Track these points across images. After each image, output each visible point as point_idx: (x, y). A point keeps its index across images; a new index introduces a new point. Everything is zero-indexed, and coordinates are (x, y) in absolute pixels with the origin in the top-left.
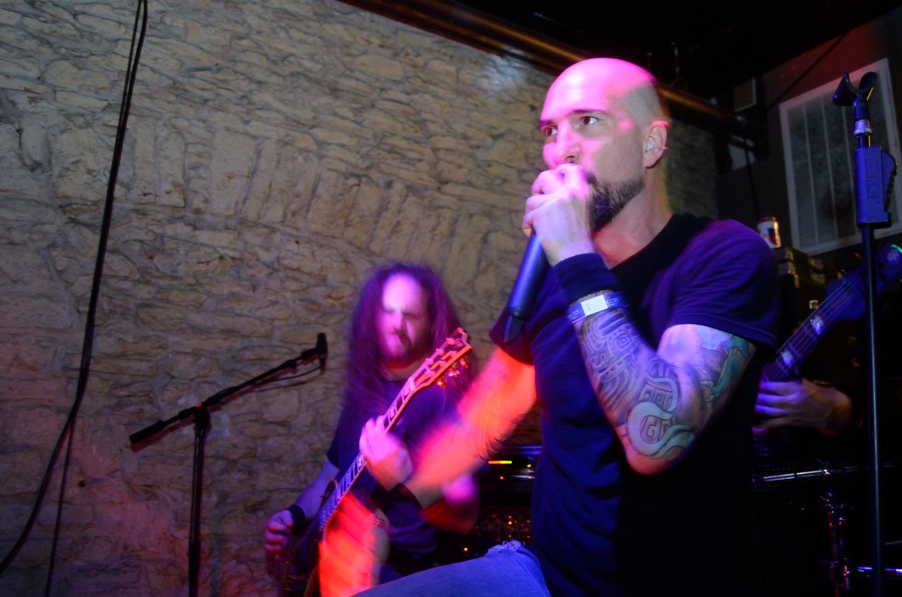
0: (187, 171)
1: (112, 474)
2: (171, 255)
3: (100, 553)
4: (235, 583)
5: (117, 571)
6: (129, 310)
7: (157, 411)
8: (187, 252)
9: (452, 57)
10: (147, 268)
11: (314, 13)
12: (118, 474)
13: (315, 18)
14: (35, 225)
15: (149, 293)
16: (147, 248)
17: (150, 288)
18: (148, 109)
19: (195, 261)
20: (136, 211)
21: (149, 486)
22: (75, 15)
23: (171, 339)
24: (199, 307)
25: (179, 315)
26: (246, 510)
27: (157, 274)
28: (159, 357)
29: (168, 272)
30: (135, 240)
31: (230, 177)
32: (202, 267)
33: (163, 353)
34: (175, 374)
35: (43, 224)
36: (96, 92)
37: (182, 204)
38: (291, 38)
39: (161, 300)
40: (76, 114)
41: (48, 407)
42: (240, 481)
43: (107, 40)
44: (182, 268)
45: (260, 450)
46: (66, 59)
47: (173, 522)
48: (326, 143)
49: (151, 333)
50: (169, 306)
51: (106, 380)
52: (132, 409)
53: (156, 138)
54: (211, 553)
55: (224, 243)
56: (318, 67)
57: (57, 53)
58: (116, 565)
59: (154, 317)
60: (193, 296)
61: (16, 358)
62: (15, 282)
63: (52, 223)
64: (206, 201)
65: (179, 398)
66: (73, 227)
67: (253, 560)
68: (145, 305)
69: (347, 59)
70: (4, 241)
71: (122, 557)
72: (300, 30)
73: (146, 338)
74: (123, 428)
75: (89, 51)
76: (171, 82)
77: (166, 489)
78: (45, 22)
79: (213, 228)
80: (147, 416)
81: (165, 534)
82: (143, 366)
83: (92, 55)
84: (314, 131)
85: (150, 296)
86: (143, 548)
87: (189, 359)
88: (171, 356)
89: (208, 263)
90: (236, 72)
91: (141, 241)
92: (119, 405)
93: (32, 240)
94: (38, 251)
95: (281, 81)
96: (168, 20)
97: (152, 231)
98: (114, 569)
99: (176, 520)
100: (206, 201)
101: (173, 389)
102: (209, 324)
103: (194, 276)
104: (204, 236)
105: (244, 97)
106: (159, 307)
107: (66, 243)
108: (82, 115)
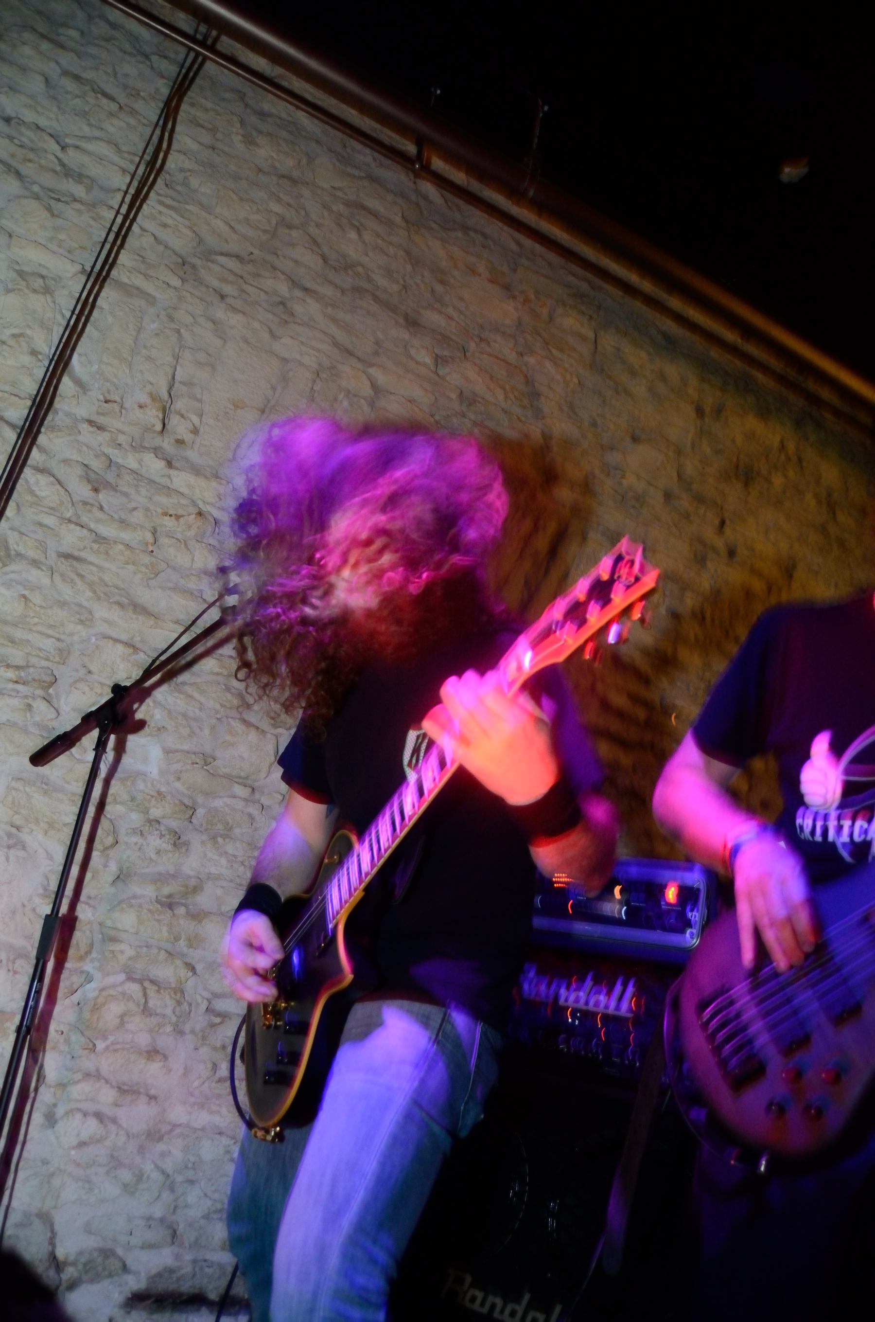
0: (177, 385)
2: (126, 495)
4: (113, 1011)
7: (53, 714)
9: (591, 317)
11: (403, 217)
13: (404, 224)
15: (81, 539)
16: (92, 475)
18: (138, 289)
19: (160, 511)
20: (91, 422)
21: (18, 828)
22: (63, 148)
26: (158, 901)
31: (236, 407)
32: (169, 522)
36: (69, 252)
37: (159, 427)
38: (364, 242)
40: (34, 274)
43: (102, 188)
44: (137, 518)
45: (201, 812)
46: (37, 197)
47: (41, 891)
48: (387, 391)
53: (140, 330)
54: (88, 953)
55: (209, 496)
56: (395, 288)
57: (26, 188)
64: (195, 431)
67: (152, 982)
69: (439, 288)
72: (378, 235)
73: (62, 604)
75: (72, 195)
76: (180, 260)
77: (40, 837)
78: (21, 146)
79: (197, 471)
80: (37, 718)
81: (24, 906)
82: (48, 644)
83: (75, 200)
84: (372, 371)
88: (93, 639)
89: (178, 517)
90: (275, 269)
95: (339, 294)
96: (194, 182)
100: (195, 431)
101: (87, 689)
103: (154, 532)
104: (181, 480)
105: (282, 303)
108: (43, 277)
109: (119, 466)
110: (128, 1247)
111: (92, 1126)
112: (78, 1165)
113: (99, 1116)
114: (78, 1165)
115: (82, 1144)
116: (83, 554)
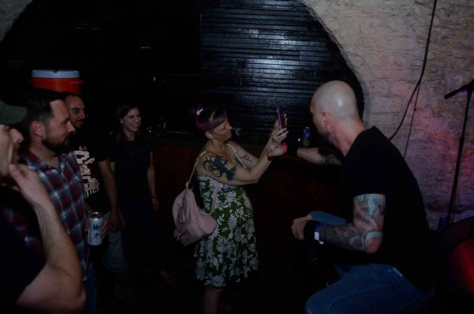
1: (427, 106)
2: (457, 14)
3: (420, 135)
4: (469, 152)
5: (426, 142)
6: (438, 40)
8: (464, 13)
10: (447, 21)
12: (429, 107)
14: (402, 6)
15: (447, 32)
17: (447, 30)
23: (454, 51)
25: (458, 41)
27: (451, 23)
28: (448, 60)
29: (456, 22)
30: (442, 8)
32: (470, 18)
33: (450, 58)
34: (454, 67)
35: (405, 6)
39: (452, 35)
41: (404, 80)
44: (462, 19)
49: (445, 50)
50: (454, 37)
51: (427, 70)
52: (437, 81)
58: (425, 140)
59: (448, 43)
60: (466, 32)
61: (394, 62)
62: (394, 31)
63: (408, 5)
65: (455, 77)
66: (417, 6)
68: (444, 38)
70: (391, 15)
71: (428, 138)
74: (432, 89)
82: (442, 64)
85: (447, 33)
87: (461, 60)
88: (453, 59)
91: (444, 9)
92: (431, 80)
93: (400, 13)
94: (403, 17)
97: (449, 3)
98: (425, 142)
99: (449, 125)
103: (467, 23)
106: (450, 38)
107: (414, 13)
109: (453, 5)
111: (466, 178)
112: (464, 186)
114: (464, 186)
115: (464, 182)
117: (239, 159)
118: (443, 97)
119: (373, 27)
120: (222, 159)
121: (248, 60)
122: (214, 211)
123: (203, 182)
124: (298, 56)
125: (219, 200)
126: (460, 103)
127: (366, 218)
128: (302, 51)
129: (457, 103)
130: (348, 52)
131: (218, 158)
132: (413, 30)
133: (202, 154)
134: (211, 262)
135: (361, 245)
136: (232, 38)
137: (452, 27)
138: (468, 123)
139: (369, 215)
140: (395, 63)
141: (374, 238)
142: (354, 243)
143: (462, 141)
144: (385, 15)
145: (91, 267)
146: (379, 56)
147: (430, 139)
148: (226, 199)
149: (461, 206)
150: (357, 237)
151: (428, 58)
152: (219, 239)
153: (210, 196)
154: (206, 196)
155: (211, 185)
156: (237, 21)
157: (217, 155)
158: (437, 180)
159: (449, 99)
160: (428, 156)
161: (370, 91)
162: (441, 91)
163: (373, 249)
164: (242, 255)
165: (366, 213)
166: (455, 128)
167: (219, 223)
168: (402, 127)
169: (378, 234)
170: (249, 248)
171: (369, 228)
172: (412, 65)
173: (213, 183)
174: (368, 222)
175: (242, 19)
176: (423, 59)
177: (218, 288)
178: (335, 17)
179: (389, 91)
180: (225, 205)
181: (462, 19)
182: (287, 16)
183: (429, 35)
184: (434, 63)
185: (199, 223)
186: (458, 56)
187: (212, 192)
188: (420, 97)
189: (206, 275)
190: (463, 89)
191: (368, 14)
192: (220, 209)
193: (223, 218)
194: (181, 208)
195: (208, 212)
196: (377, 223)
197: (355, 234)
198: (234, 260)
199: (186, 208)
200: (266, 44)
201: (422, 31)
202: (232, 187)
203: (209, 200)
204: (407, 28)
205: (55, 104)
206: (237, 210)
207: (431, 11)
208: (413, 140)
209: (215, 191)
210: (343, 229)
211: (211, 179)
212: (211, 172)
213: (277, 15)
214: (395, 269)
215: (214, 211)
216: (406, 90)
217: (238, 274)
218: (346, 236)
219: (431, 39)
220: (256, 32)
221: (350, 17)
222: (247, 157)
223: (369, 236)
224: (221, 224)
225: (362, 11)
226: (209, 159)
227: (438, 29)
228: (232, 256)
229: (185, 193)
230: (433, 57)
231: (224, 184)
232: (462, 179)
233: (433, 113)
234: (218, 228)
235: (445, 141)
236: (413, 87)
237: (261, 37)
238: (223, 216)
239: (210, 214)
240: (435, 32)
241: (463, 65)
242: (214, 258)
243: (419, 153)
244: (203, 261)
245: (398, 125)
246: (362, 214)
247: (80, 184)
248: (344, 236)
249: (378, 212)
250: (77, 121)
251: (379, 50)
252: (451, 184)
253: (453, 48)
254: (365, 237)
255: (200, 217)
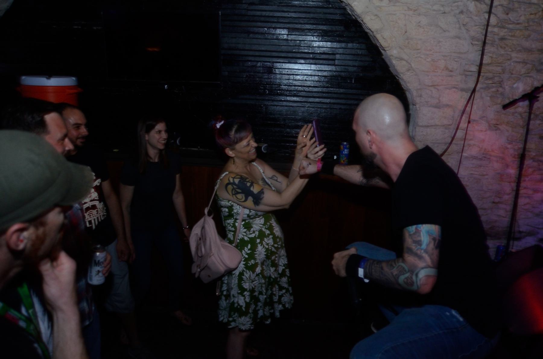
1: (482, 118)
3: (474, 151)
4: (531, 170)
5: (481, 159)
14: (454, 3)
15: (505, 32)
17: (506, 30)
23: (514, 55)
24: (527, 37)
27: (510, 22)
29: (516, 22)
30: (499, 5)
32: (532, 16)
34: (514, 72)
39: (512, 36)
41: (456, 88)
42: (539, 124)
49: (503, 52)
50: (513, 38)
51: (483, 76)
52: (494, 90)
59: (507, 45)
60: (527, 33)
62: (445, 31)
68: (502, 39)
71: (483, 154)
74: (489, 98)
82: (499, 69)
86: (493, 151)
89: (535, 14)
91: (502, 5)
92: (487, 88)
93: (452, 10)
94: (455, 16)
99: (508, 140)
102: (533, 46)
103: (528, 22)
107: (468, 10)
110: (538, 228)
111: (527, 200)
113: (529, 197)
116: (506, 37)
117: (266, 180)
118: (499, 107)
119: (421, 27)
120: (247, 180)
121: (275, 65)
122: (238, 241)
123: (225, 207)
124: (334, 60)
125: (245, 228)
126: (520, 114)
127: (419, 252)
128: (338, 54)
129: (516, 114)
130: (392, 56)
131: (243, 179)
132: (467, 30)
133: (223, 175)
134: (236, 301)
135: (412, 284)
136: (257, 38)
137: (511, 26)
138: (529, 137)
139: (422, 249)
140: (447, 69)
141: (428, 276)
142: (404, 281)
143: (522, 157)
144: (434, 12)
145: (93, 308)
146: (428, 60)
147: (485, 156)
148: (252, 227)
149: (520, 232)
150: (407, 275)
151: (484, 62)
152: (245, 274)
153: (234, 224)
154: (229, 224)
155: (235, 211)
156: (262, 19)
157: (241, 176)
158: (494, 202)
159: (508, 110)
160: (484, 175)
161: (418, 100)
162: (499, 101)
163: (426, 289)
164: (272, 291)
165: (419, 247)
166: (514, 143)
167: (244, 255)
168: (454, 142)
169: (432, 272)
170: (281, 283)
171: (421, 264)
172: (465, 71)
173: (237, 209)
174: (420, 257)
175: (268, 17)
176: (478, 62)
177: (245, 331)
178: (376, 15)
179: (439, 100)
180: (251, 234)
181: (523, 18)
182: (320, 13)
183: (486, 36)
184: (490, 68)
185: (221, 256)
186: (518, 60)
187: (236, 219)
188: (475, 107)
189: (230, 316)
190: (524, 97)
191: (415, 11)
192: (246, 238)
193: (249, 250)
194: (200, 239)
195: (231, 242)
196: (431, 259)
197: (405, 271)
198: (262, 298)
199: (205, 239)
200: (296, 46)
201: (477, 31)
202: (259, 213)
203: (233, 229)
204: (460, 28)
205: (51, 118)
206: (265, 239)
207: (487, 8)
208: (466, 157)
209: (240, 218)
210: (391, 265)
211: (235, 204)
212: (234, 196)
213: (309, 13)
214: (454, 312)
215: (238, 241)
216: (458, 99)
217: (267, 314)
218: (394, 274)
219: (487, 41)
220: (284, 32)
221: (395, 14)
222: (275, 178)
223: (422, 274)
224: (247, 256)
225: (408, 8)
226: (231, 180)
227: (496, 30)
228: (261, 293)
229: (205, 220)
230: (490, 62)
231: (250, 210)
232: (522, 201)
233: (490, 126)
234: (244, 261)
235: (503, 159)
236: (467, 95)
237: (290, 37)
238: (249, 246)
239: (234, 245)
240: (492, 32)
241: (523, 71)
242: (240, 296)
243: (473, 172)
244: (226, 300)
245: (450, 139)
246: (414, 247)
247: (80, 211)
248: (392, 273)
249: (432, 246)
250: (77, 138)
251: (428, 53)
252: (509, 208)
253: (512, 51)
254: (417, 275)
255: (222, 250)
